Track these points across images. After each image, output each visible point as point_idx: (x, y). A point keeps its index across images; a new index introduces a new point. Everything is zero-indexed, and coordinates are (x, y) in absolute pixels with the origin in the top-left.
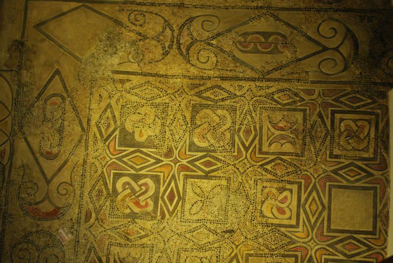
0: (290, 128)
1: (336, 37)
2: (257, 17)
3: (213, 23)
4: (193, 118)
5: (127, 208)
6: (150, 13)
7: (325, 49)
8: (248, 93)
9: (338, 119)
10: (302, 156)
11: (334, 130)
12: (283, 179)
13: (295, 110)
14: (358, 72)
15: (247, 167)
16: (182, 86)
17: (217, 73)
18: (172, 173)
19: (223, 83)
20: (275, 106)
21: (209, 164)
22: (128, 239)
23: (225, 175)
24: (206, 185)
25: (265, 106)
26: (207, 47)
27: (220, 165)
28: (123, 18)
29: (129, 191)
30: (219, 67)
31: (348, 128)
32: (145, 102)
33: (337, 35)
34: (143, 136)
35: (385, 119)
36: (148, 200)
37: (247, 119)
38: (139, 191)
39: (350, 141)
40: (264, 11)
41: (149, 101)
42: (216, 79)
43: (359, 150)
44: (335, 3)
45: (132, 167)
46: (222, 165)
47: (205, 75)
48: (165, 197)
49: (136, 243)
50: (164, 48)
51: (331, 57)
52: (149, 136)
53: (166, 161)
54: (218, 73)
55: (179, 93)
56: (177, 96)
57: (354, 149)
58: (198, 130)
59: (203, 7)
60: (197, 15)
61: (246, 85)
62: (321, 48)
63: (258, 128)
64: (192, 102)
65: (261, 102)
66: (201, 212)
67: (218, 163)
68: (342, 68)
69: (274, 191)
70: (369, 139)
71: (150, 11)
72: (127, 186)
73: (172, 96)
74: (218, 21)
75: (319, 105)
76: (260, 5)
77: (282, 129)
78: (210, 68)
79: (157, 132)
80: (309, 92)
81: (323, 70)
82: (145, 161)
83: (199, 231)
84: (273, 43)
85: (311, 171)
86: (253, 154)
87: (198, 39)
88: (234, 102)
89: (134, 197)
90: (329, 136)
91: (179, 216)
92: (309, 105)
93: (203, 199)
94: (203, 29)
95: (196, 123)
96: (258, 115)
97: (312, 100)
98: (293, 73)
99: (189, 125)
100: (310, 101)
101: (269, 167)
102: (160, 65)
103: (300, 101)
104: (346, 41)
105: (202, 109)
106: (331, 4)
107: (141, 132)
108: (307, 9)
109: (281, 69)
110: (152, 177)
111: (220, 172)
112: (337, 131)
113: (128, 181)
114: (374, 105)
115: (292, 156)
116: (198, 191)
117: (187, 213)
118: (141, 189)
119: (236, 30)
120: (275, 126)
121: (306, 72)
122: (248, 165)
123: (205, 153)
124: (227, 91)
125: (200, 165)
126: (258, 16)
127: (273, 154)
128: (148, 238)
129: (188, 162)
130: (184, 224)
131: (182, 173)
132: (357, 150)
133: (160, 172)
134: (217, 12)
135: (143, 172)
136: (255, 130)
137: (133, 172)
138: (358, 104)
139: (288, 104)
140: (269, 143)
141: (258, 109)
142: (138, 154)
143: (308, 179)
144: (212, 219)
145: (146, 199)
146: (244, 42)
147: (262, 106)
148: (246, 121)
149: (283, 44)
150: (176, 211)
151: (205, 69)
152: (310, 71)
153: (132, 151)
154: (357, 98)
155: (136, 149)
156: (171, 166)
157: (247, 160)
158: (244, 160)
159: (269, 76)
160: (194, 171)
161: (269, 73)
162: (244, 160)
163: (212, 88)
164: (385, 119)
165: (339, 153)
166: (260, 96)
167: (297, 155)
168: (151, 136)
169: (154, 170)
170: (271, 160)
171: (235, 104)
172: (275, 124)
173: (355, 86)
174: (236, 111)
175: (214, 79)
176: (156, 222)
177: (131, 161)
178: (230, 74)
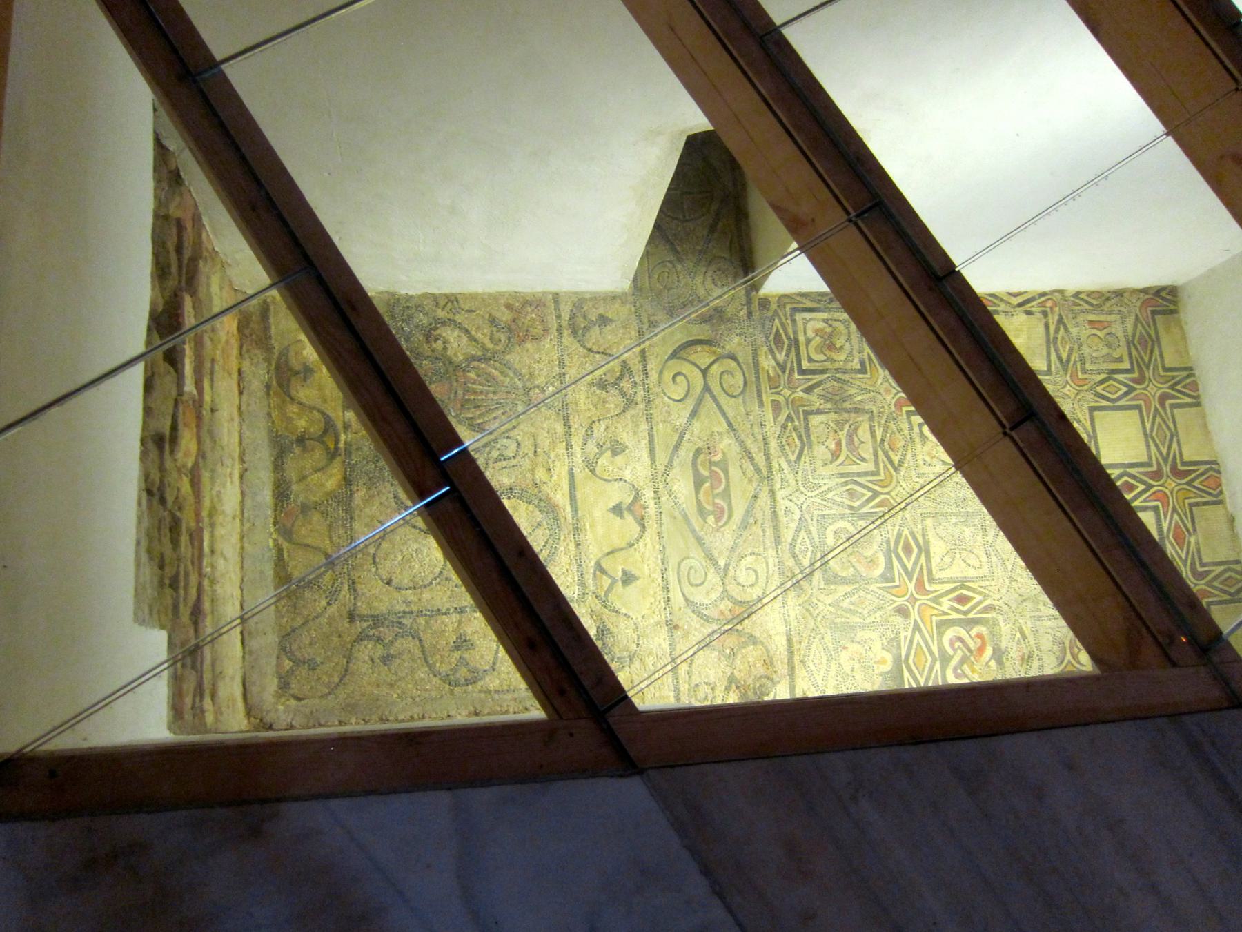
0: (836, 432)
1: (687, 375)
2: (673, 496)
3: (691, 568)
4: (845, 581)
5: (989, 667)
6: (690, 677)
7: (707, 388)
8: (794, 499)
9: (808, 364)
10: (872, 412)
11: (827, 369)
12: (909, 437)
13: (807, 429)
14: (737, 339)
15: (902, 491)
16: (800, 605)
17: (771, 552)
18: (929, 603)
19: (786, 541)
20: (807, 458)
21: (908, 550)
22: (1030, 657)
23: (920, 522)
25: (809, 472)
26: (731, 573)
27: (906, 532)
29: (965, 667)
30: (762, 548)
31: (819, 349)
32: (834, 662)
33: (684, 372)
34: (883, 658)
35: (799, 299)
36: (973, 635)
37: (834, 498)
38: (963, 652)
39: (838, 346)
40: (661, 486)
41: (831, 655)
42: (780, 552)
43: (849, 333)
44: (633, 377)
45: (931, 670)
46: (905, 529)
47: (776, 569)
48: (964, 608)
49: (1032, 643)
50: (744, 645)
51: (718, 379)
52: (883, 649)
53: (914, 615)
54: (770, 550)
55: (811, 609)
56: (817, 612)
57: (848, 340)
58: (862, 570)
59: (666, 589)
60: (681, 595)
61: (783, 504)
62: (708, 396)
63: (844, 480)
64: (822, 587)
65: (805, 479)
66: (975, 551)
67: (904, 535)
68: (734, 364)
69: (926, 448)
70: (831, 320)
71: (687, 676)
72: (959, 671)
73: (819, 619)
74: (688, 560)
75: (793, 392)
76: (652, 494)
77: (839, 444)
78: (764, 565)
79: (874, 635)
80: (777, 407)
81: (740, 390)
82: (919, 649)
83: (1000, 551)
84: (710, 469)
85: (889, 398)
86: (880, 483)
87: (721, 589)
88: (812, 520)
89: (972, 658)
90: (837, 375)
91: (987, 583)
92: (795, 408)
93: (957, 551)
94: (703, 583)
95: (853, 576)
96: (826, 481)
97: (787, 404)
98: (753, 435)
99: (857, 585)
100: (790, 406)
101: (896, 459)
102: (772, 647)
103: (792, 421)
104: (691, 358)
105: (830, 568)
106: (636, 383)
107: (878, 662)
108: (649, 418)
109: (750, 453)
110: (940, 634)
111: (915, 530)
112: (828, 365)
113: (951, 671)
114: (781, 314)
115: (874, 426)
116: (948, 559)
117: (981, 573)
118: (959, 647)
119: (697, 529)
120: (835, 455)
121: (747, 414)
122: (899, 489)
123: (893, 555)
124: (798, 530)
125: (912, 562)
126: (670, 496)
127: (876, 455)
128: (1023, 627)
129: (910, 580)
130: (996, 574)
131: (928, 587)
132: (849, 336)
133: (931, 622)
134: (673, 562)
135: (935, 649)
136: (846, 483)
137: (938, 666)
138: (783, 336)
139: (800, 438)
140: (862, 461)
141: (816, 481)
142: (911, 661)
144: (981, 534)
145: (971, 637)
146: (715, 515)
147: (810, 477)
148: (836, 498)
149: (710, 453)
150: (982, 590)
151: (767, 572)
152: (745, 410)
153: (909, 672)
154: (775, 338)
155: (903, 665)
156: (920, 605)
157: (891, 491)
158: (891, 496)
159: (764, 469)
160: (921, 569)
161: (758, 470)
162: (891, 496)
163: (795, 556)
164: (799, 299)
165: (856, 360)
166: (797, 481)
167: (871, 419)
168: (883, 644)
169: (930, 630)
170: (886, 457)
171: (815, 519)
172: (832, 454)
173: (759, 343)
174: (824, 515)
175: (780, 556)
176: (1000, 618)
177: (923, 671)
178: (769, 532)
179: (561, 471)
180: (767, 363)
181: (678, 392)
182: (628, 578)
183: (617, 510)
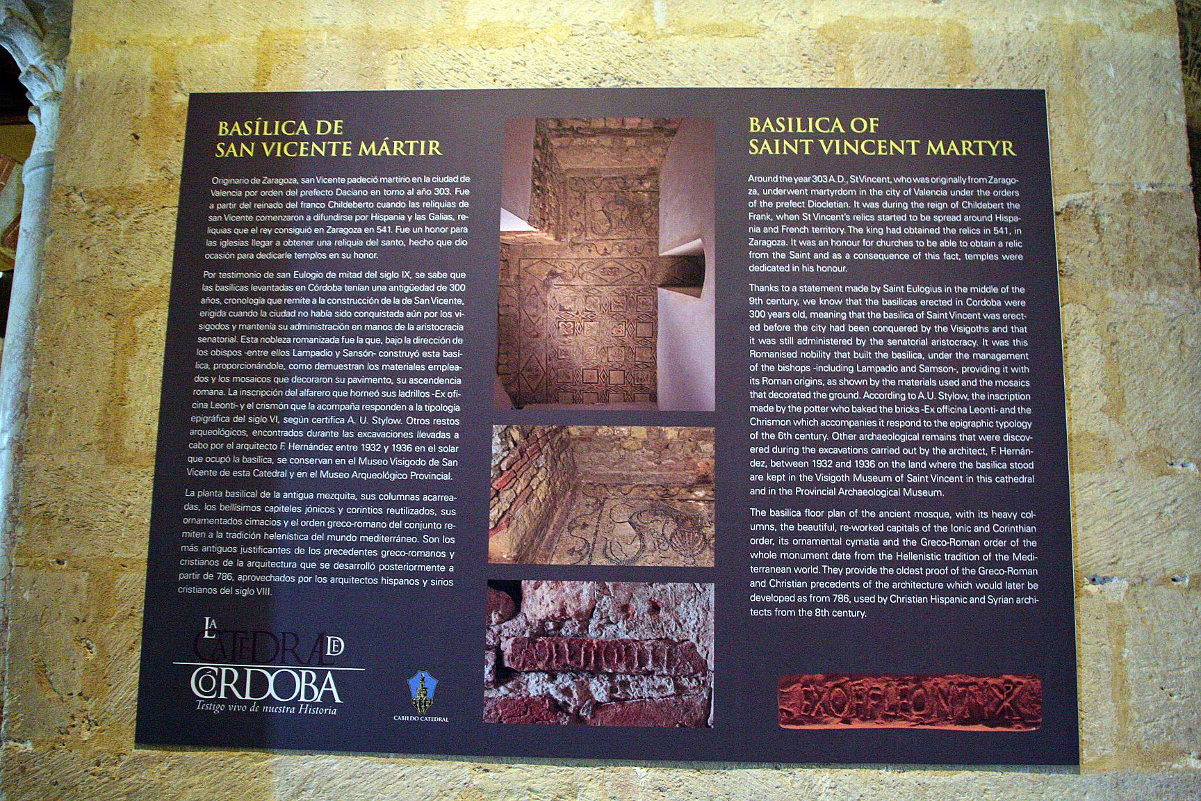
24: (592, 324)
28: (557, 265)
80: (628, 289)
143: (628, 320)
179: (615, 237)
180: (640, 288)
181: (633, 266)
182: (590, 251)
183: (606, 249)
